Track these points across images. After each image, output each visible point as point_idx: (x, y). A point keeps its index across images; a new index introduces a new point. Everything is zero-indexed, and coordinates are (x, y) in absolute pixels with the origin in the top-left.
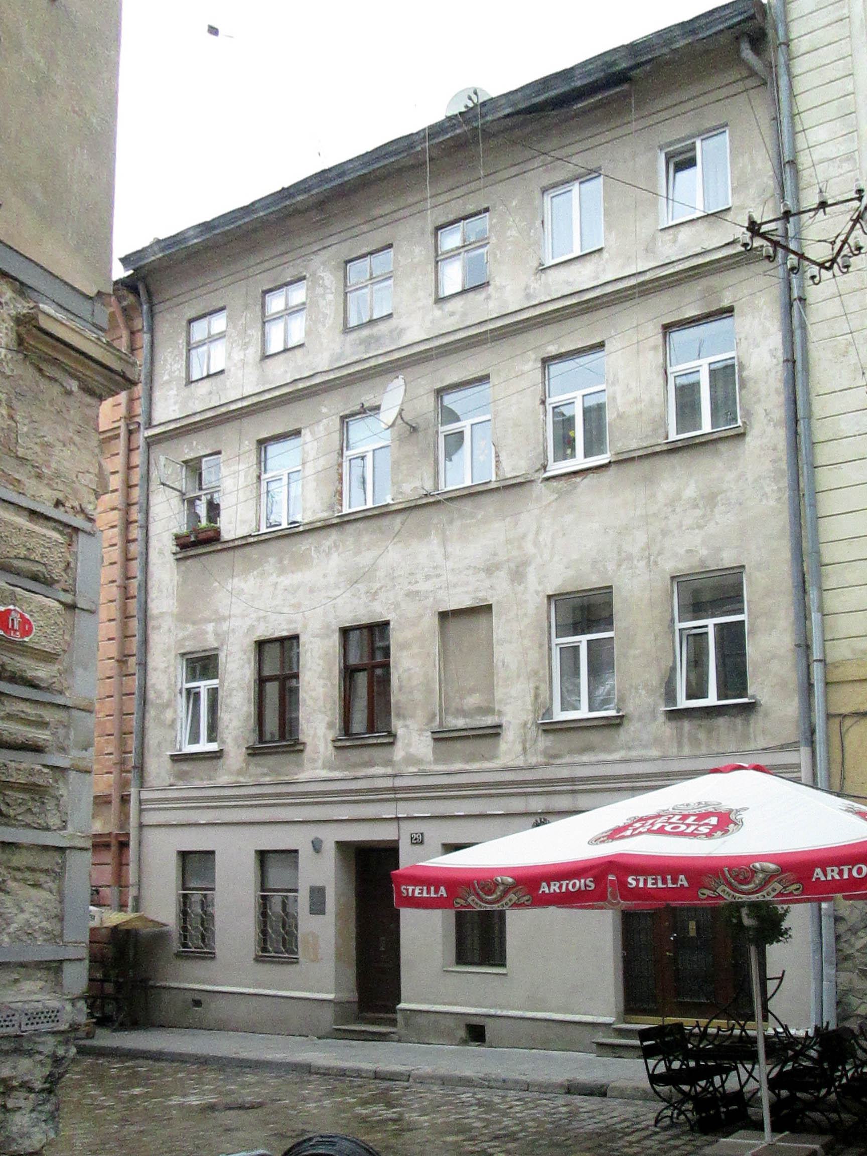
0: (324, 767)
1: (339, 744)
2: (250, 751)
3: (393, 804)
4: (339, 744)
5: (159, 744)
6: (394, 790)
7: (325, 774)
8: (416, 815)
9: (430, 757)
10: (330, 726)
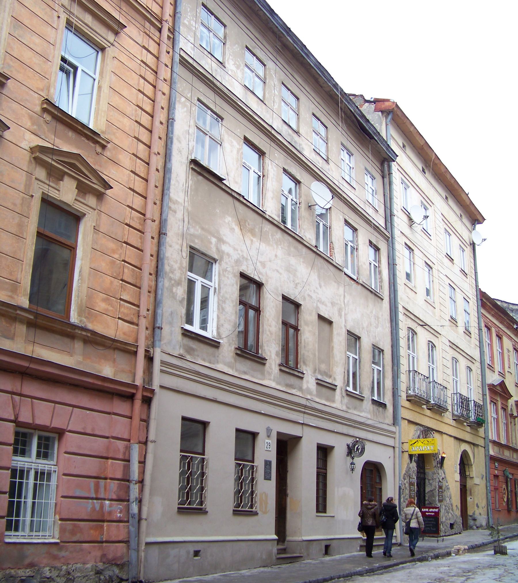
0: (274, 381)
1: (283, 368)
2: (239, 352)
3: (302, 415)
4: (283, 368)
5: (172, 313)
6: (305, 407)
7: (273, 384)
8: (311, 424)
9: (315, 392)
10: (277, 355)
